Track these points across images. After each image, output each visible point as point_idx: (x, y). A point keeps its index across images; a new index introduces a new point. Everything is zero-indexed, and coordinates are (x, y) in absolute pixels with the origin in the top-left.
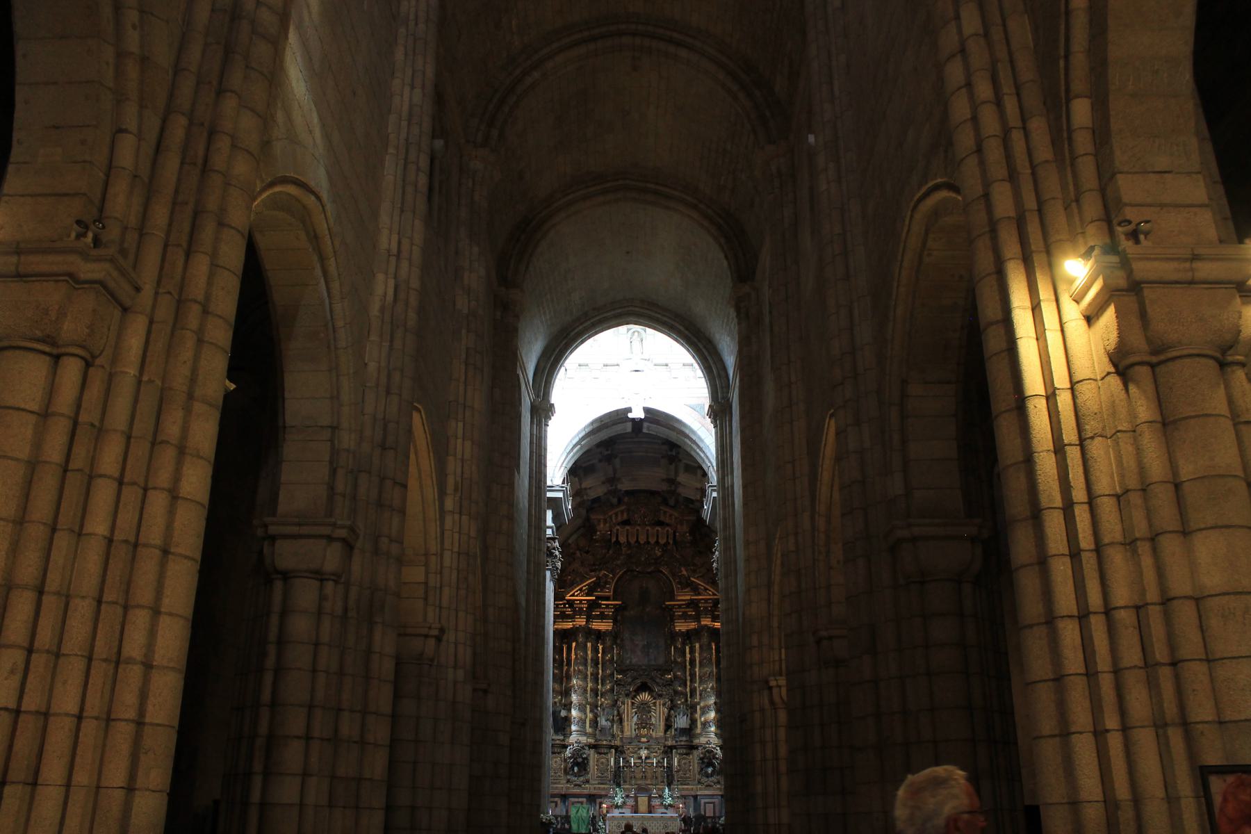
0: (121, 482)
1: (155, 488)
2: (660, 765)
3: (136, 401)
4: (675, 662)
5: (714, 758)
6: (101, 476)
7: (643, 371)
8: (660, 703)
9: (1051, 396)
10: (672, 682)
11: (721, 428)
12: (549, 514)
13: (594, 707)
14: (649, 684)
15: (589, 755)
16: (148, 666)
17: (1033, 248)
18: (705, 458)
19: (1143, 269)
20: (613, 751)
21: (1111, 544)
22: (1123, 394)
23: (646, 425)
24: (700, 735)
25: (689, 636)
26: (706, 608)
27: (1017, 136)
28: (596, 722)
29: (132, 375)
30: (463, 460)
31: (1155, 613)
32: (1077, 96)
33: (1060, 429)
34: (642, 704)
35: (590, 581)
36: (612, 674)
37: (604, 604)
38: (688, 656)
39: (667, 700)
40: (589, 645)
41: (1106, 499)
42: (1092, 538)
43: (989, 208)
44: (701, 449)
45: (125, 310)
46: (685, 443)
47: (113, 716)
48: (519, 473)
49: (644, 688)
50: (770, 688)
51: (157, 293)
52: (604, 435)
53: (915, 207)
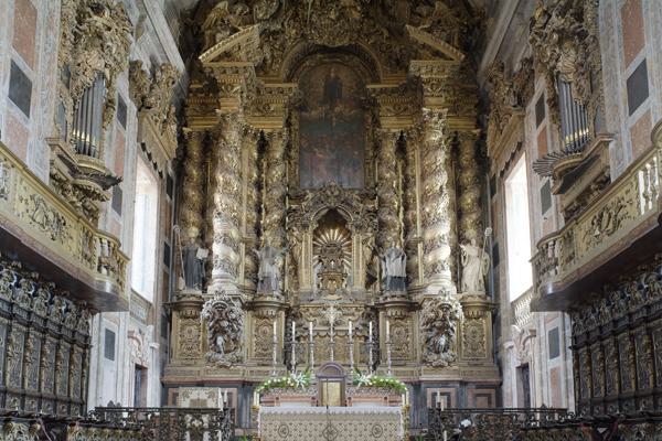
2: (358, 333)
4: (380, 178)
10: (376, 212)
14: (341, 212)
20: (283, 314)
28: (257, 271)
39: (370, 234)
40: (245, 153)
49: (333, 219)
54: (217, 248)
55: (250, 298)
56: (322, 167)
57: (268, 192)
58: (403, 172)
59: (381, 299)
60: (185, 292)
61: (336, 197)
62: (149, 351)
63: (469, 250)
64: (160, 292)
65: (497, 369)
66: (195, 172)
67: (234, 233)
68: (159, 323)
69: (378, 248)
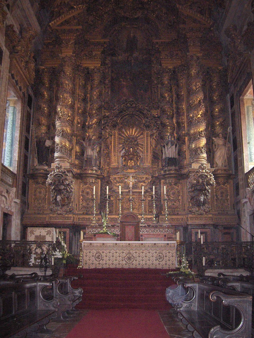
5: (208, 184)
8: (147, 134)
20: (100, 180)
38: (175, 96)
39: (155, 131)
40: (77, 80)
54: (57, 140)
55: (79, 171)
56: (125, 90)
57: (91, 105)
59: (162, 172)
60: (37, 167)
61: (133, 107)
62: (13, 204)
63: (219, 141)
64: (22, 168)
65: (237, 217)
66: (45, 93)
67: (68, 130)
68: (20, 187)
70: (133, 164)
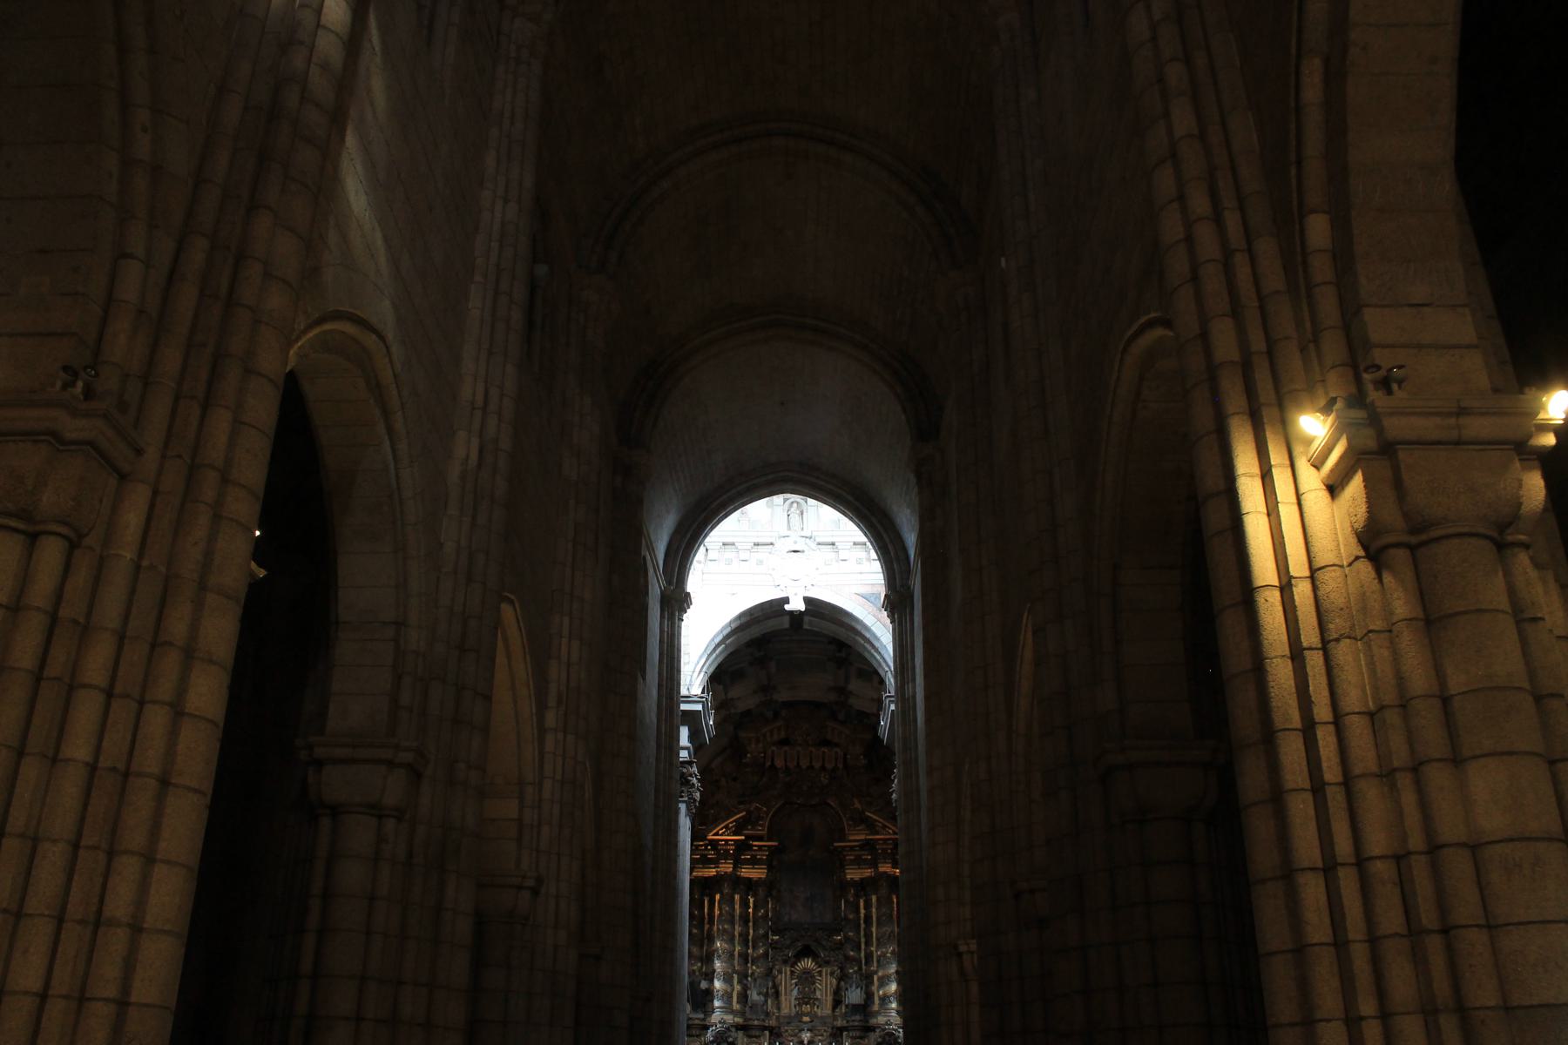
0: (109, 694)
1: (154, 702)
3: (133, 591)
4: (846, 919)
6: (85, 686)
7: (803, 551)
8: (827, 971)
9: (1286, 587)
11: (900, 624)
12: (684, 733)
13: (743, 976)
14: (813, 948)
15: (736, 1038)
16: (136, 929)
17: (1262, 400)
18: (881, 661)
19: (1396, 427)
20: (767, 1033)
21: (1363, 776)
22: (1375, 585)
23: (806, 619)
24: (878, 1013)
25: (863, 887)
26: (884, 851)
27: (1240, 260)
28: (746, 997)
29: (128, 558)
30: (569, 665)
31: (1419, 868)
32: (1313, 211)
33: (1297, 630)
34: (804, 973)
35: (738, 816)
36: (766, 936)
37: (756, 846)
38: (862, 911)
39: (836, 968)
40: (737, 897)
41: (1355, 718)
42: (1340, 768)
43: (1208, 352)
44: (877, 650)
45: (123, 477)
46: (857, 642)
47: (88, 995)
48: (644, 679)
49: (806, 952)
50: (960, 955)
51: (164, 457)
52: (756, 632)
53: (1125, 350)
58: (865, 909)
59: (845, 1022)
60: (690, 1016)
69: (843, 977)
70: (809, 1010)
